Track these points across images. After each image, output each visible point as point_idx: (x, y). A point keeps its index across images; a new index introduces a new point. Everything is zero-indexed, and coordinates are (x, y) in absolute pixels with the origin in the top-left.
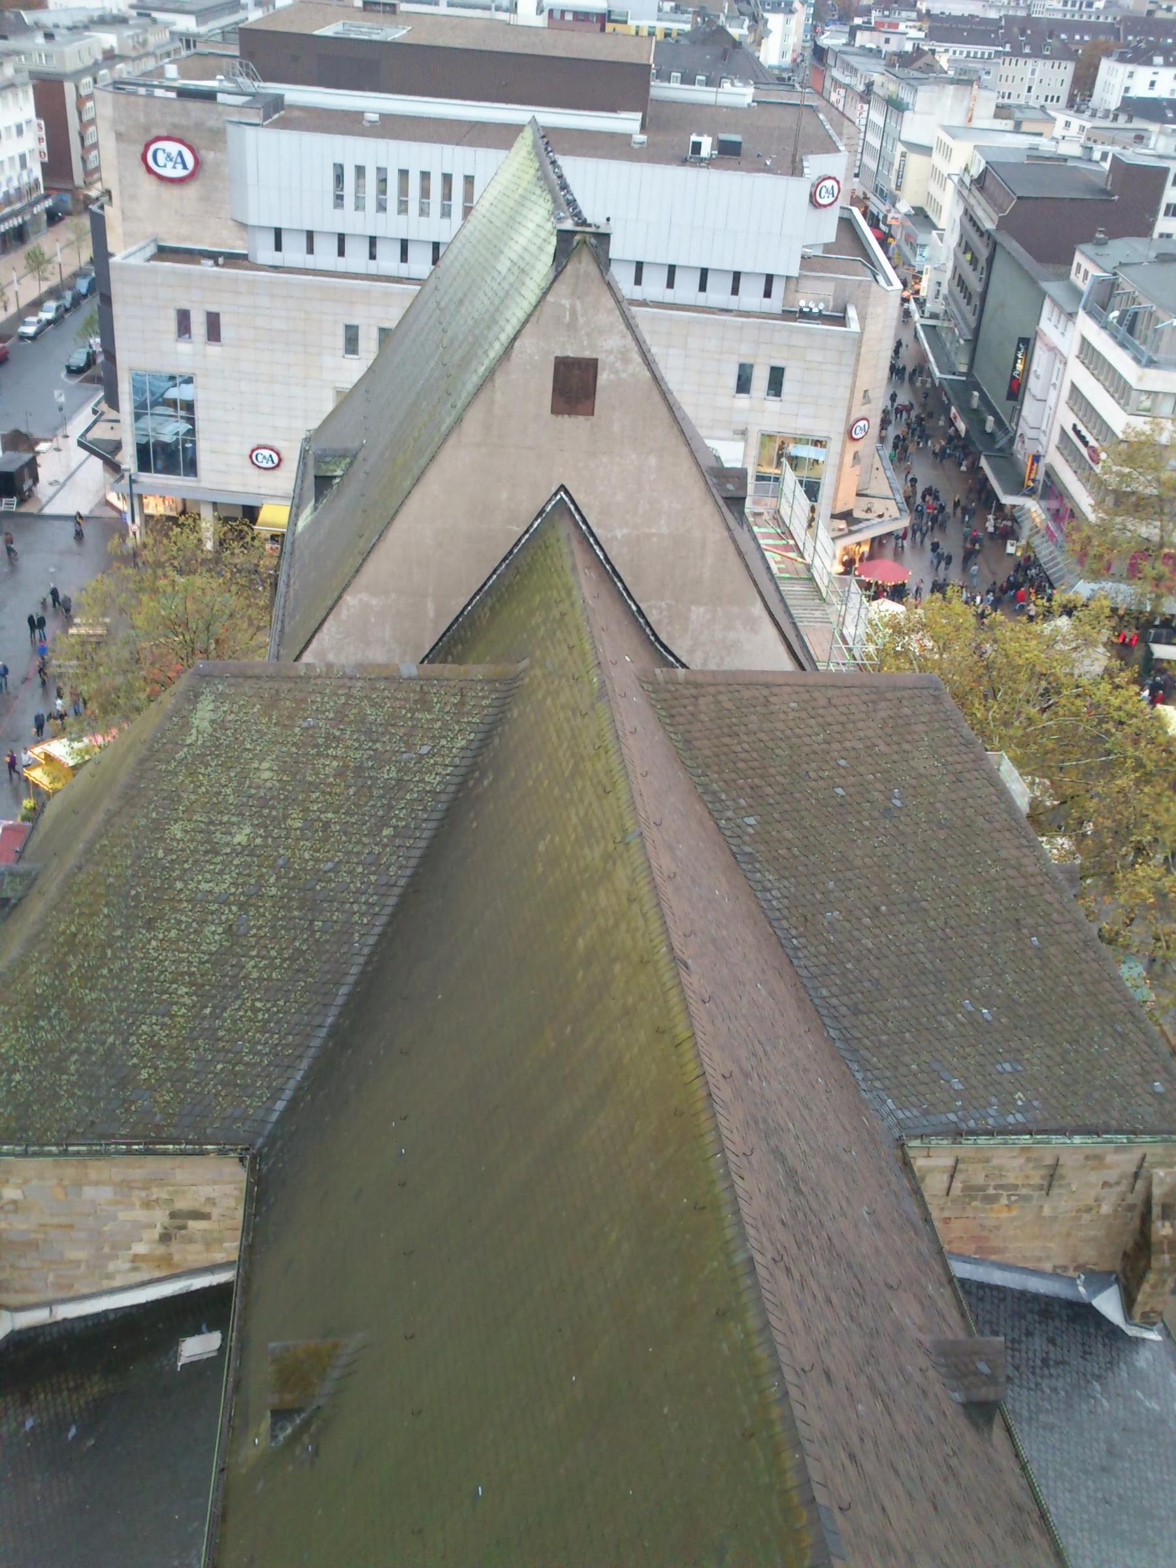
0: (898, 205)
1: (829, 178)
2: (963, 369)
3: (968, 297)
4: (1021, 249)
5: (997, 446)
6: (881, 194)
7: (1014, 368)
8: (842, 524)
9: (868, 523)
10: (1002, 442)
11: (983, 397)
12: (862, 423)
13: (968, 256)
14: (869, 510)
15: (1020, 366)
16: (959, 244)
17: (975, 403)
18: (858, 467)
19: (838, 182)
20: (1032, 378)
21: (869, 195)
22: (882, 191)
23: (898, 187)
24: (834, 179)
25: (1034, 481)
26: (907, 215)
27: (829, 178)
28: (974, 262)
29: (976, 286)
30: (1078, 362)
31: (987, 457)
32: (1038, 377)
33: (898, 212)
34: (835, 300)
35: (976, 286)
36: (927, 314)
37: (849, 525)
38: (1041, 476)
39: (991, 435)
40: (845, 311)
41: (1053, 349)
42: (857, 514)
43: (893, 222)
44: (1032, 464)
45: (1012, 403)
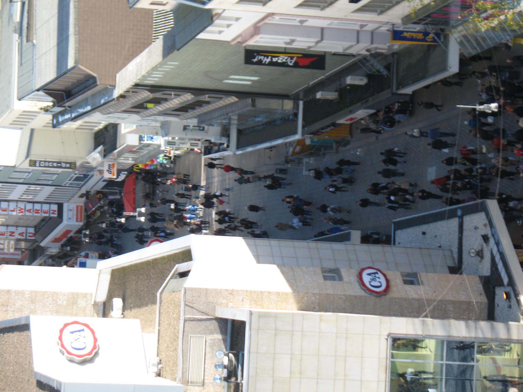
0: (94, 164)
1: (60, 338)
2: (288, 105)
3: (199, 104)
4: (137, 60)
5: (385, 72)
6: (85, 177)
7: (283, 65)
8: (501, 295)
9: (498, 258)
10: (379, 67)
11: (321, 85)
12: (366, 279)
13: (150, 105)
14: (480, 254)
15: (281, 59)
16: (137, 113)
17: (331, 95)
18: (423, 276)
19: (66, 325)
20: (295, 45)
21: (83, 191)
22: (77, 179)
23: (72, 165)
24: (61, 331)
25: (426, 34)
26: (105, 154)
27: (60, 338)
28: (157, 101)
29: (188, 97)
30: (269, 4)
31: (402, 84)
32: (293, 41)
33: (102, 165)
34: (212, 333)
35: (188, 97)
36: (224, 140)
37: (501, 284)
38: (418, 27)
39: (370, 77)
40: (223, 322)
41: (256, 29)
42: (486, 270)
43: (115, 170)
44: (405, 39)
45: (328, 61)
